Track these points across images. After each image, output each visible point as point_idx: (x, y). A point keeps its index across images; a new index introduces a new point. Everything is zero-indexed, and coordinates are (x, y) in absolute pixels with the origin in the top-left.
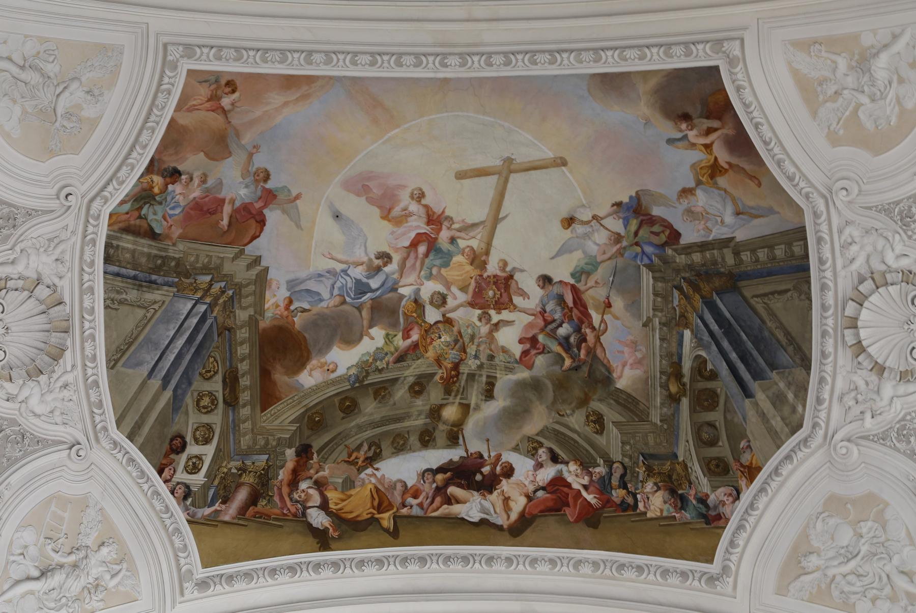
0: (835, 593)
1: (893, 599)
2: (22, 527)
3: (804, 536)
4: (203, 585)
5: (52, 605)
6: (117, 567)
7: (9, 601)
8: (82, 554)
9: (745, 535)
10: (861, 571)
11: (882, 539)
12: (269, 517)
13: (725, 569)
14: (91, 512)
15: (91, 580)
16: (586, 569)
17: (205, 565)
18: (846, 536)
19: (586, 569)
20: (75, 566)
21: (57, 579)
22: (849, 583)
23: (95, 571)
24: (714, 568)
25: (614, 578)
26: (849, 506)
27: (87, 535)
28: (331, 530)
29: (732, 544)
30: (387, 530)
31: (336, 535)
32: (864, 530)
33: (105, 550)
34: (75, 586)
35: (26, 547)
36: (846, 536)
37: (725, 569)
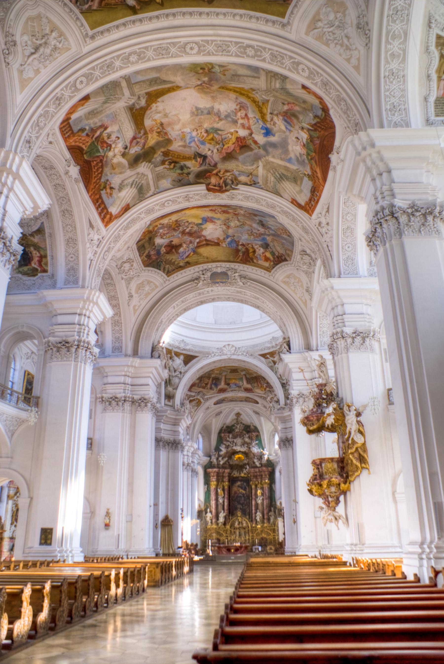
0: (325, 39)
1: (342, 45)
2: (22, 35)
3: (318, 13)
4: (93, 37)
5: (43, 60)
6: (60, 39)
7: (29, 65)
8: (46, 38)
9: (297, 9)
10: (334, 32)
11: (343, 22)
12: (111, 4)
13: (288, 22)
14: (44, 20)
15: (53, 47)
16: (238, 18)
17: (92, 29)
18: (332, 17)
19: (238, 18)
20: (46, 43)
21: (41, 50)
22: (329, 36)
23: (53, 43)
24: (285, 20)
25: (247, 21)
26: (335, 5)
27: (45, 29)
28: (137, 6)
29: (292, 13)
30: (159, 3)
31: (139, 8)
32: (338, 16)
33: (54, 34)
34: (48, 51)
35: (26, 42)
36: (332, 17)
37: (288, 22)
